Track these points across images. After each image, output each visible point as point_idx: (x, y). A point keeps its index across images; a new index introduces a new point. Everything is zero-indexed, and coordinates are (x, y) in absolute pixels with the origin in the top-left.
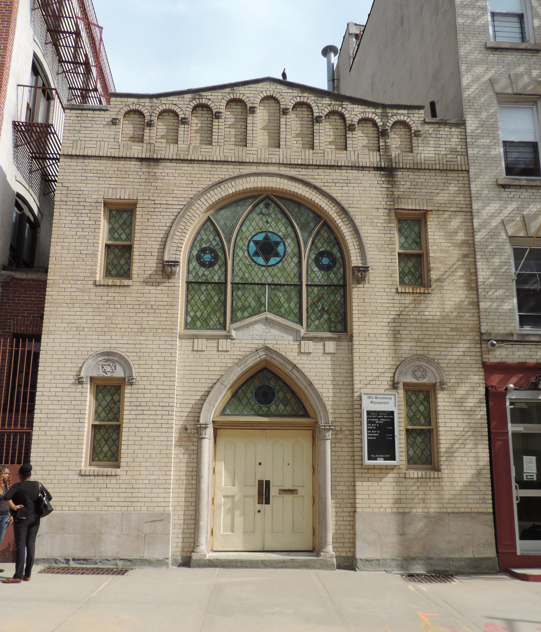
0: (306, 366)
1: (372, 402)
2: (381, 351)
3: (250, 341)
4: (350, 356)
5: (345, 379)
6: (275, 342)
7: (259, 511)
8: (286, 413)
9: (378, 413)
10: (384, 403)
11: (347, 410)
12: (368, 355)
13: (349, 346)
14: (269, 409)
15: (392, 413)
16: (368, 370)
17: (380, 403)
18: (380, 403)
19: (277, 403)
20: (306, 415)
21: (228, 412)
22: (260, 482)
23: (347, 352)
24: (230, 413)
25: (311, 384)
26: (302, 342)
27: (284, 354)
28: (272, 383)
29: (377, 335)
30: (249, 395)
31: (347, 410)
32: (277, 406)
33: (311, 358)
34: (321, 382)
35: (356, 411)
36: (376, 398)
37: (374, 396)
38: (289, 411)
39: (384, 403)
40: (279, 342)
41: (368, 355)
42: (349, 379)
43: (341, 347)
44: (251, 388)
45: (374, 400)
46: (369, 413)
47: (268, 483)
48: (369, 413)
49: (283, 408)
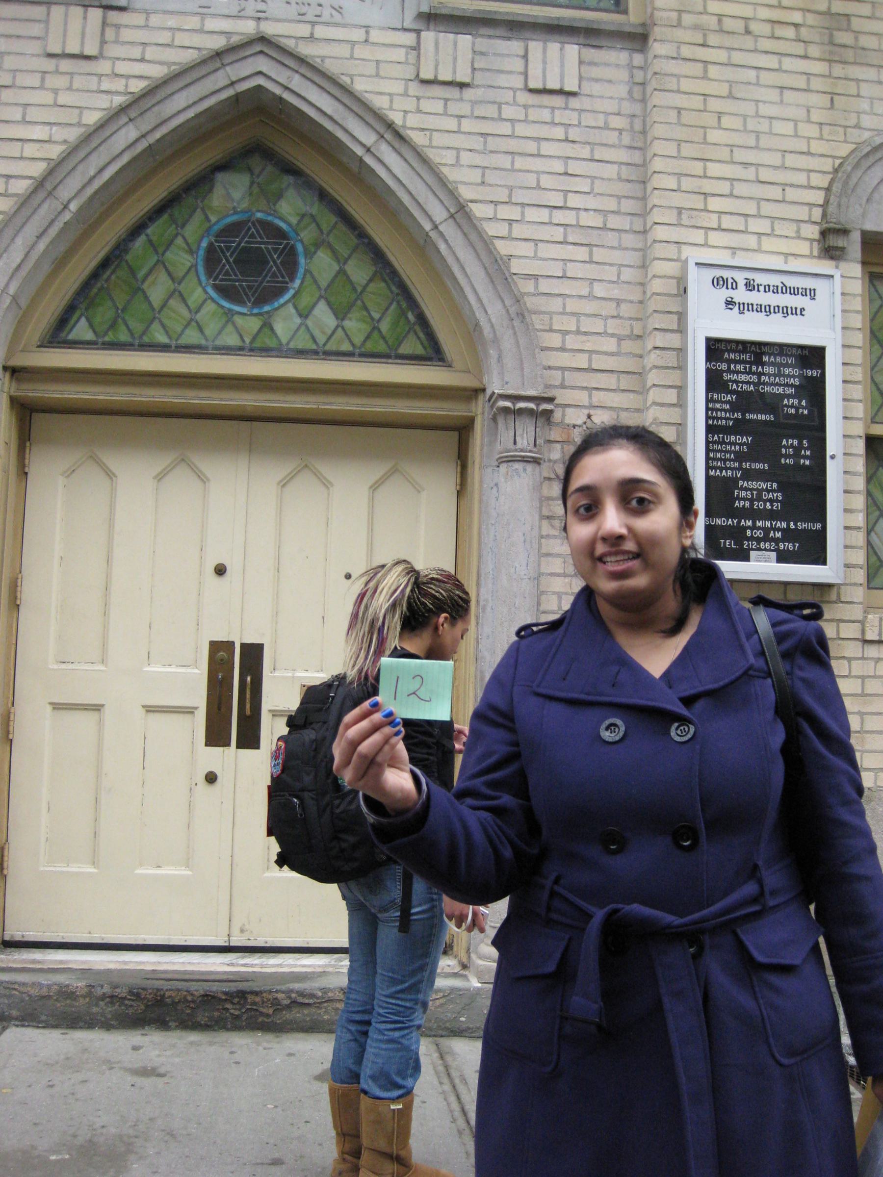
0: (439, 139)
1: (730, 303)
2: (774, 95)
3: (193, 22)
4: (637, 109)
5: (611, 204)
6: (304, 30)
7: (211, 778)
8: (346, 347)
9: (756, 351)
10: (787, 311)
11: (620, 339)
12: (714, 105)
13: (631, 67)
14: (267, 326)
15: (812, 357)
16: (714, 169)
17: (768, 310)
18: (768, 310)
19: (305, 300)
20: (434, 354)
21: (81, 330)
22: (219, 652)
23: (622, 90)
24: (89, 336)
25: (460, 212)
26: (428, 36)
27: (346, 80)
28: (290, 209)
29: (754, 27)
30: (180, 259)
31: (620, 339)
32: (304, 315)
33: (465, 109)
34: (505, 212)
35: (660, 340)
36: (750, 286)
37: (740, 277)
38: (358, 340)
39: (787, 311)
40: (321, 32)
41: (714, 105)
42: (628, 206)
43: (595, 72)
44: (192, 230)
45: (741, 295)
46: (716, 348)
47: (253, 655)
48: (716, 348)
49: (330, 321)
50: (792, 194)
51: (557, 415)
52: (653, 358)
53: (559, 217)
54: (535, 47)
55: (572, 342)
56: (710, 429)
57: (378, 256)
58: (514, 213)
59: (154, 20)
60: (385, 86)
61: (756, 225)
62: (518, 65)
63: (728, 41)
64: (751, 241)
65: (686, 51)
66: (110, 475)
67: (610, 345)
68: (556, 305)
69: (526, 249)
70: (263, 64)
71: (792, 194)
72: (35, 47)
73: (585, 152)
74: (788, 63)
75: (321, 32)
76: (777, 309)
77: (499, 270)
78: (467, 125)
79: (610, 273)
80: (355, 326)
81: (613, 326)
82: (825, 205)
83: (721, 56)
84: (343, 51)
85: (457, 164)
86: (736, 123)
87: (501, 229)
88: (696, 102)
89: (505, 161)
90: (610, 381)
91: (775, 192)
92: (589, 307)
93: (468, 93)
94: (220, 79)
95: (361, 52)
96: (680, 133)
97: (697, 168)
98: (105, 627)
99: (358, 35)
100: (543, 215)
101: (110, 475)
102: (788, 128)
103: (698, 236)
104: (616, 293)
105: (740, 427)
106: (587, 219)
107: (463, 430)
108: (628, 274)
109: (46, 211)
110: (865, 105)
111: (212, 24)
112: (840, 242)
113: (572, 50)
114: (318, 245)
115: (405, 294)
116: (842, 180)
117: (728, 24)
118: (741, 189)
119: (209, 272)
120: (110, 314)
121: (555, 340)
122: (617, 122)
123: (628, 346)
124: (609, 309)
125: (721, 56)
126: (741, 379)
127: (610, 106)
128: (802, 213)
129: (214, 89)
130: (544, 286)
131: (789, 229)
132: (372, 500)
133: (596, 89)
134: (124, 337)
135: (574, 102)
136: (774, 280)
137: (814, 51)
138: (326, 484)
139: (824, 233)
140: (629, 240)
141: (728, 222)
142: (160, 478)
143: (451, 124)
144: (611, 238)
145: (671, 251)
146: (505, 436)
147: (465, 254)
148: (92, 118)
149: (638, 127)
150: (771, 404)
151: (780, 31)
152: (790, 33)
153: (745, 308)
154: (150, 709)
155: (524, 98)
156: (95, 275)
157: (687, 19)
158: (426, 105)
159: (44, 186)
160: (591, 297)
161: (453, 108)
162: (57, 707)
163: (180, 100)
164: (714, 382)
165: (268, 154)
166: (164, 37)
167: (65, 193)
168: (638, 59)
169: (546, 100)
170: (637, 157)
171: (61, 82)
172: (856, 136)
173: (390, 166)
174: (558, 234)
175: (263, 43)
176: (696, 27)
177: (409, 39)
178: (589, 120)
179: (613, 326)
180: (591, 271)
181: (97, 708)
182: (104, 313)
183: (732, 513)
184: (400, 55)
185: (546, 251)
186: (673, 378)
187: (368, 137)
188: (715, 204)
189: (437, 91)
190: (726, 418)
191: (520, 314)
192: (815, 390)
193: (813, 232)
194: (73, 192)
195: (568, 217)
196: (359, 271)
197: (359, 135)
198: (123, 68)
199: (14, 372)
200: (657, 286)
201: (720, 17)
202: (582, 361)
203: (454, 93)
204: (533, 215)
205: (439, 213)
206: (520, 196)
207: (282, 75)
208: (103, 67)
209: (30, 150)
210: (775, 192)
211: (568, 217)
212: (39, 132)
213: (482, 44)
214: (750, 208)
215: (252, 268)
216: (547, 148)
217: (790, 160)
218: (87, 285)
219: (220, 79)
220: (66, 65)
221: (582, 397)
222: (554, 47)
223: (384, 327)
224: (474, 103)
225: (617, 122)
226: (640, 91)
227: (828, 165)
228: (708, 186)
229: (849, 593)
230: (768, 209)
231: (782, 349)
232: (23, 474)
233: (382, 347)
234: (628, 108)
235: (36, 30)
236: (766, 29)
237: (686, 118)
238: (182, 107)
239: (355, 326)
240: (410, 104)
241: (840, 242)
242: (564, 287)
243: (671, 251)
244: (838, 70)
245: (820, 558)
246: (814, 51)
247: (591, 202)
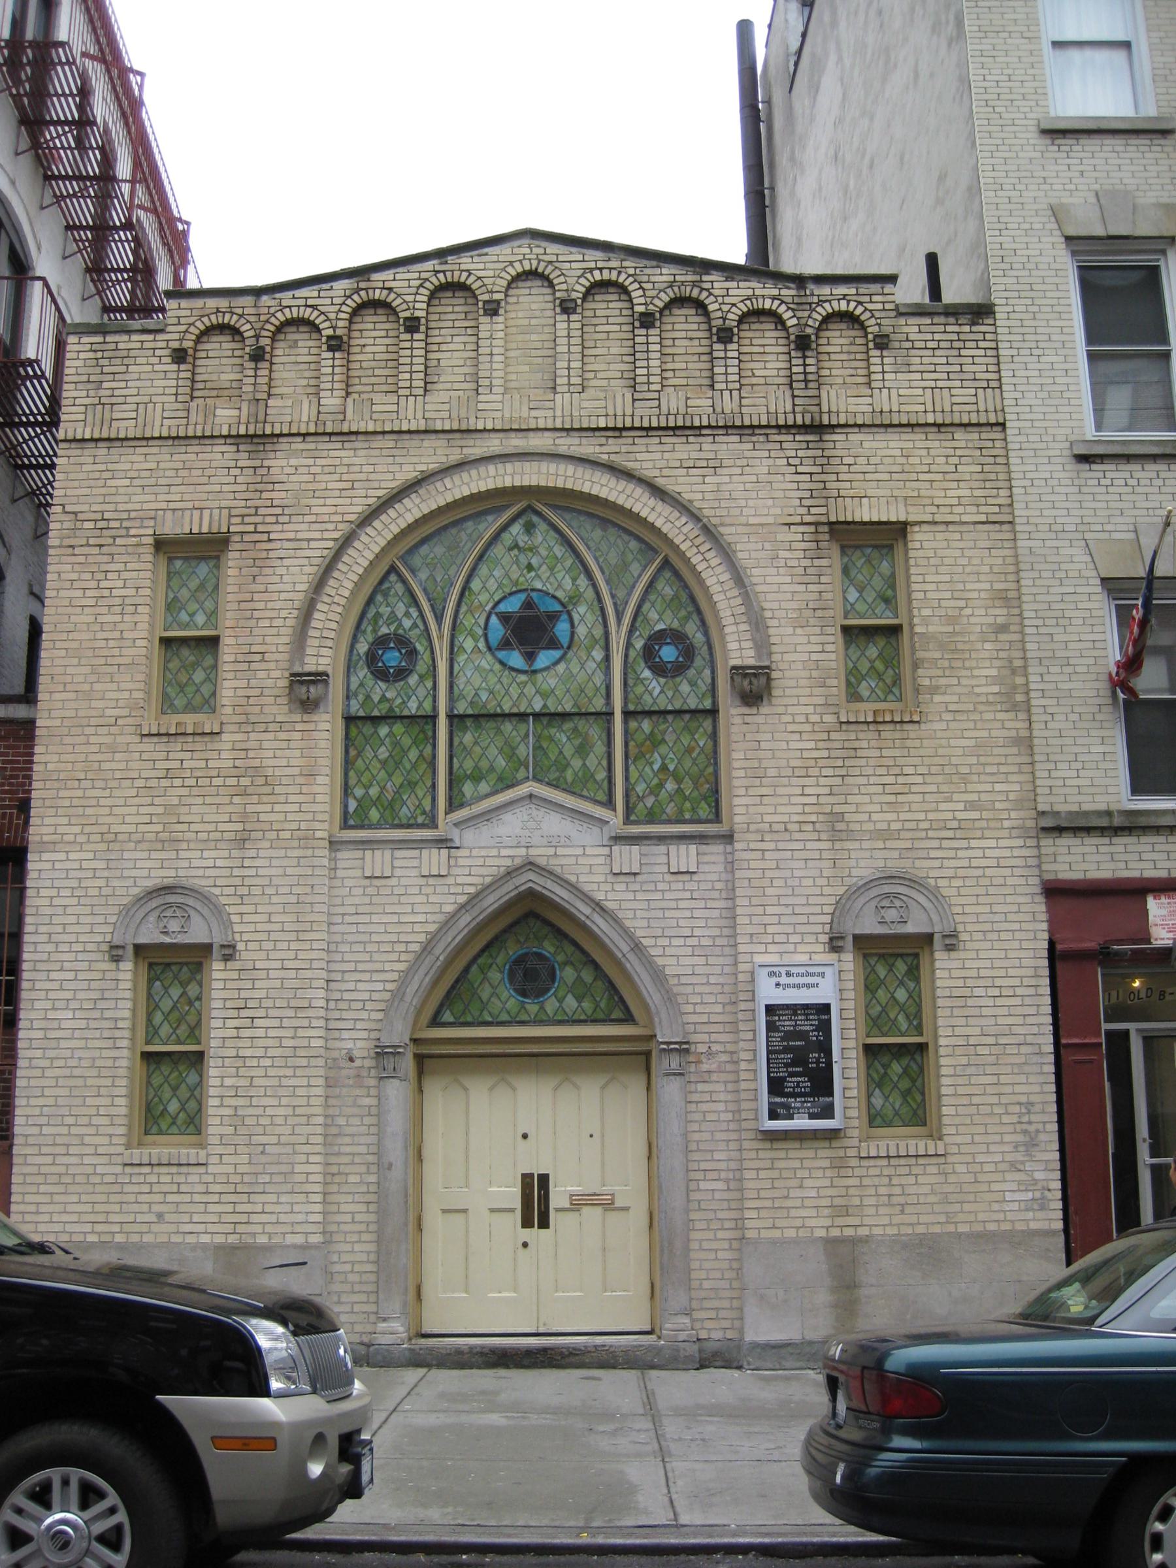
0: (624, 905)
1: (778, 985)
2: (801, 864)
3: (494, 852)
4: (729, 877)
5: (717, 932)
6: (551, 851)
7: (525, 1245)
8: (583, 1017)
9: (793, 1009)
10: (809, 986)
11: (724, 1005)
12: (769, 874)
13: (725, 853)
14: (542, 1008)
15: (826, 1008)
16: (769, 910)
17: (799, 986)
18: (799, 986)
19: (561, 994)
20: (629, 1019)
21: (447, 1017)
22: (527, 1178)
23: (721, 868)
24: (452, 1019)
25: (637, 947)
26: (616, 848)
27: (573, 879)
28: (548, 948)
29: (789, 826)
30: (495, 975)
31: (724, 1005)
32: (561, 1001)
33: (638, 887)
34: (661, 942)
35: (743, 1006)
36: (788, 974)
37: (783, 970)
38: (589, 1012)
39: (809, 986)
40: (560, 851)
41: (769, 874)
42: (726, 932)
43: (706, 859)
44: (500, 959)
45: (784, 980)
46: (770, 1009)
47: (544, 1179)
48: (770, 1009)
49: (574, 1004)
50: (812, 919)
51: (693, 1048)
52: (741, 1016)
53: (690, 941)
54: (673, 849)
55: (699, 1009)
56: (769, 1052)
57: (596, 966)
58: (666, 942)
59: (475, 852)
60: (595, 882)
61: (795, 938)
62: (664, 859)
63: (776, 837)
64: (791, 948)
65: (752, 846)
66: (466, 1089)
67: (719, 1008)
68: (689, 989)
69: (673, 961)
70: (531, 876)
71: (812, 919)
72: (415, 873)
73: (702, 904)
74: (809, 845)
75: (560, 851)
76: (804, 985)
77: (658, 976)
78: (639, 896)
79: (718, 970)
80: (587, 1005)
81: (720, 998)
82: (831, 923)
83: (772, 846)
84: (572, 860)
85: (635, 918)
86: (781, 883)
87: (659, 951)
88: (759, 874)
89: (660, 914)
90: (720, 1028)
91: (804, 919)
92: (707, 989)
93: (639, 878)
94: (510, 886)
95: (581, 861)
96: (750, 892)
97: (760, 910)
98: (467, 1170)
99: (579, 851)
100: (681, 942)
101: (466, 1089)
102: (810, 882)
103: (762, 948)
104: (721, 980)
105: (786, 1050)
106: (705, 942)
107: (648, 1054)
108: (727, 969)
109: (429, 960)
110: (853, 863)
111: (504, 852)
112: (840, 943)
113: (693, 848)
114: (566, 963)
115: (612, 986)
116: (841, 906)
117: (776, 827)
118: (784, 920)
119: (511, 983)
120: (462, 1007)
121: (690, 1008)
122: (719, 886)
123: (728, 1008)
124: (718, 989)
125: (772, 846)
126: (787, 1024)
127: (715, 877)
128: (819, 929)
129: (507, 892)
130: (684, 980)
131: (812, 939)
132: (602, 1098)
133: (705, 868)
134: (469, 1019)
135: (695, 877)
136: (802, 970)
137: (824, 836)
138: (578, 1088)
139: (831, 939)
140: (727, 950)
141: (777, 939)
142: (491, 1089)
143: (631, 896)
144: (718, 951)
145: (747, 958)
146: (665, 1063)
147: (639, 969)
148: (449, 909)
149: (730, 886)
150: (802, 1035)
151: (804, 827)
152: (810, 827)
153: (785, 986)
154: (492, 1210)
155: (668, 877)
156: (453, 987)
157: (753, 827)
158: (617, 887)
159: (427, 948)
160: (708, 983)
161: (632, 887)
162: (444, 1211)
163: (491, 899)
164: (771, 1027)
165: (537, 916)
166: (480, 862)
167: (437, 951)
168: (729, 848)
169: (680, 877)
170: (729, 904)
171: (430, 890)
172: (848, 881)
173: (600, 925)
174: (689, 951)
175: (530, 865)
176: (758, 831)
177: (606, 851)
178: (703, 886)
179: (720, 998)
180: (707, 970)
181: (465, 1211)
182: (459, 1007)
183: (782, 1094)
184: (601, 860)
185: (683, 961)
186: (749, 1026)
187: (587, 911)
188: (770, 929)
189: (622, 878)
190: (778, 1044)
191: (670, 998)
192: (825, 1027)
193: (824, 938)
194: (441, 951)
195: (694, 942)
196: (587, 976)
197: (582, 910)
198: (460, 880)
199: (415, 1041)
200: (741, 977)
201: (770, 824)
202: (704, 1019)
203: (631, 879)
204: (675, 942)
205: (625, 948)
206: (668, 933)
207: (541, 881)
208: (450, 880)
209: (417, 928)
210: (804, 919)
211: (694, 942)
212: (421, 918)
213: (645, 849)
214: (790, 930)
215: (531, 978)
216: (682, 904)
217: (812, 900)
218: (449, 993)
219: (510, 886)
220: (431, 881)
221: (705, 1038)
222: (683, 848)
223: (603, 1005)
224: (642, 883)
225: (719, 886)
226: (731, 866)
227: (832, 900)
228: (766, 920)
229: (849, 1133)
230: (799, 929)
231: (806, 1007)
232: (421, 1091)
233: (601, 1016)
234: (724, 876)
235: (415, 863)
236: (796, 827)
237: (754, 883)
238: (492, 902)
239: (587, 1005)
240: (608, 887)
241: (840, 943)
242: (694, 980)
243: (747, 958)
244: (838, 845)
245: (831, 1116)
246: (824, 836)
247: (707, 932)
